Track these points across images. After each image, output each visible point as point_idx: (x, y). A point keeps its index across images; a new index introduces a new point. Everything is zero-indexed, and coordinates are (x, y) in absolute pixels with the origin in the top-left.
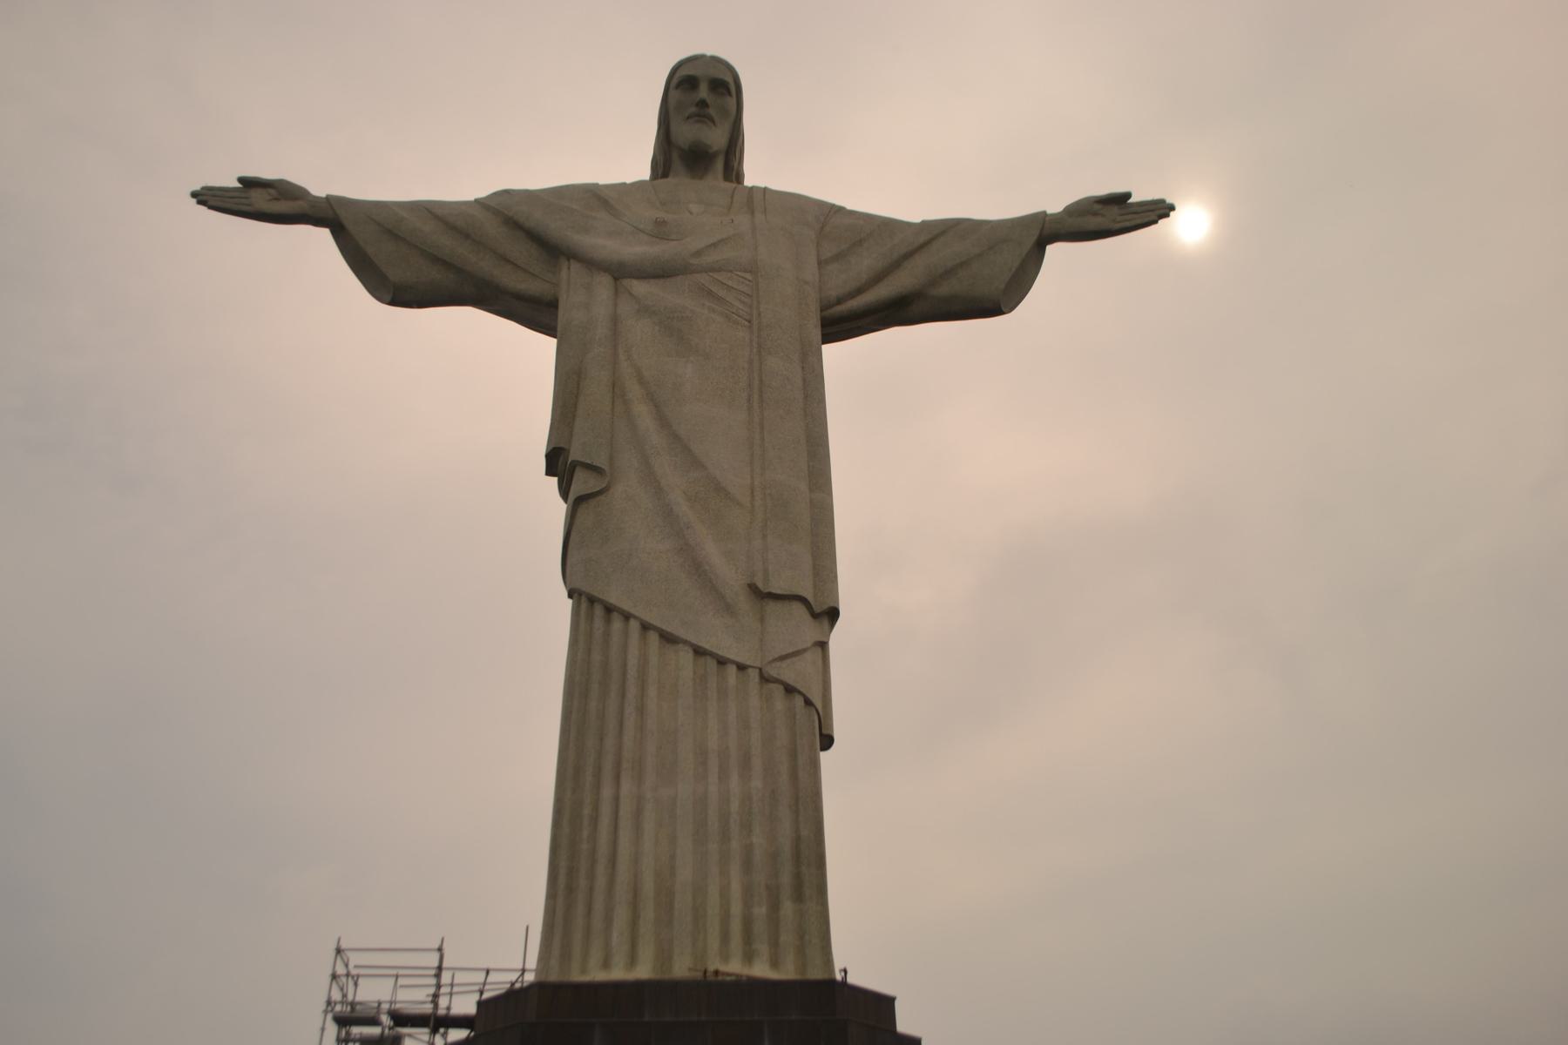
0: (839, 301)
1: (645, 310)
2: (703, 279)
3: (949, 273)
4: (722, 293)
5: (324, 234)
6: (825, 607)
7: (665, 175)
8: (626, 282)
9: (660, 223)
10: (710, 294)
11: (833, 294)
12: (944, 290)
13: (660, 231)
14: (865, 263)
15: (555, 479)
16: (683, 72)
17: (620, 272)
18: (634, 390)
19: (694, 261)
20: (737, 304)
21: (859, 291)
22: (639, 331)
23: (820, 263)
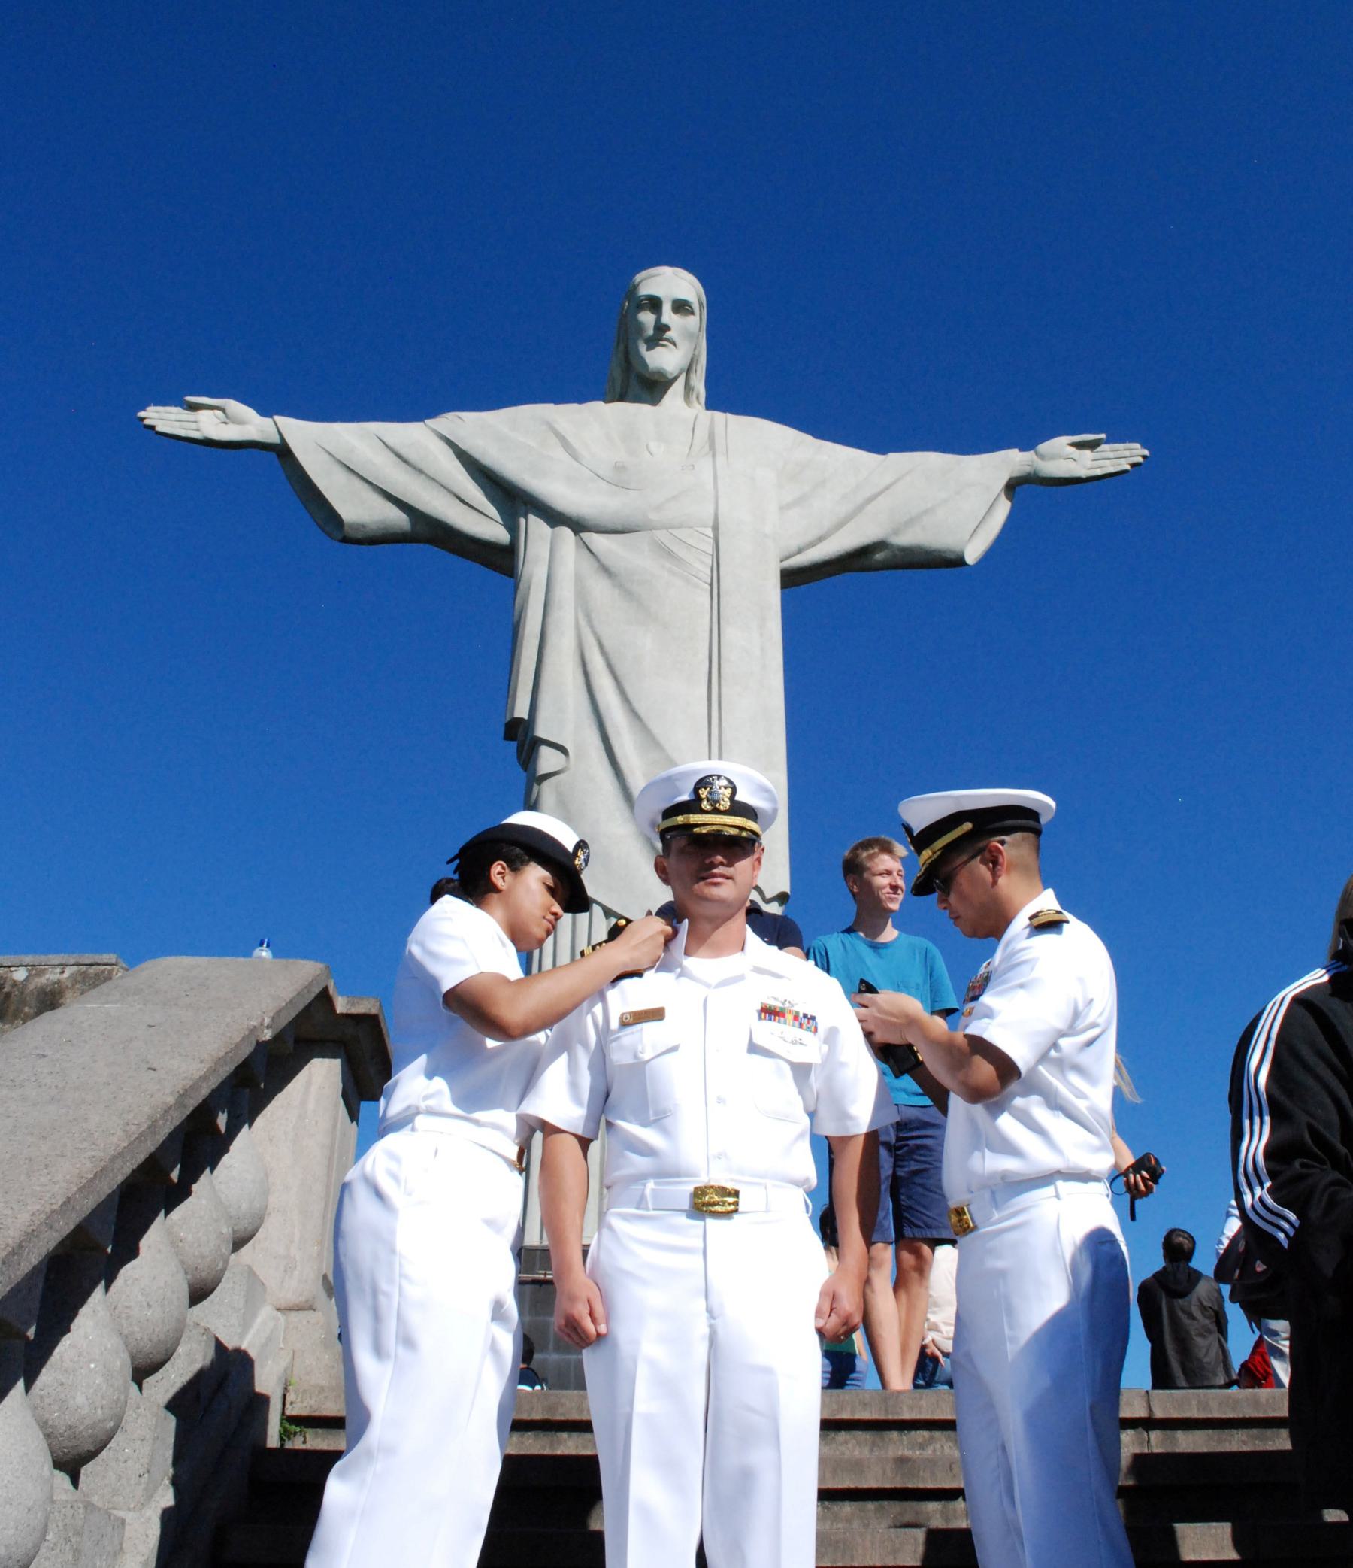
0: (799, 551)
1: (606, 570)
2: (661, 536)
3: (911, 522)
4: (681, 552)
5: (273, 455)
6: (776, 893)
7: (622, 398)
8: (585, 535)
9: (619, 468)
10: (670, 554)
11: (794, 544)
12: (905, 539)
13: (620, 478)
14: (827, 506)
15: (514, 744)
16: (645, 290)
17: (578, 526)
18: (597, 663)
19: (653, 516)
20: (697, 565)
21: (820, 539)
22: (600, 589)
23: (781, 508)
